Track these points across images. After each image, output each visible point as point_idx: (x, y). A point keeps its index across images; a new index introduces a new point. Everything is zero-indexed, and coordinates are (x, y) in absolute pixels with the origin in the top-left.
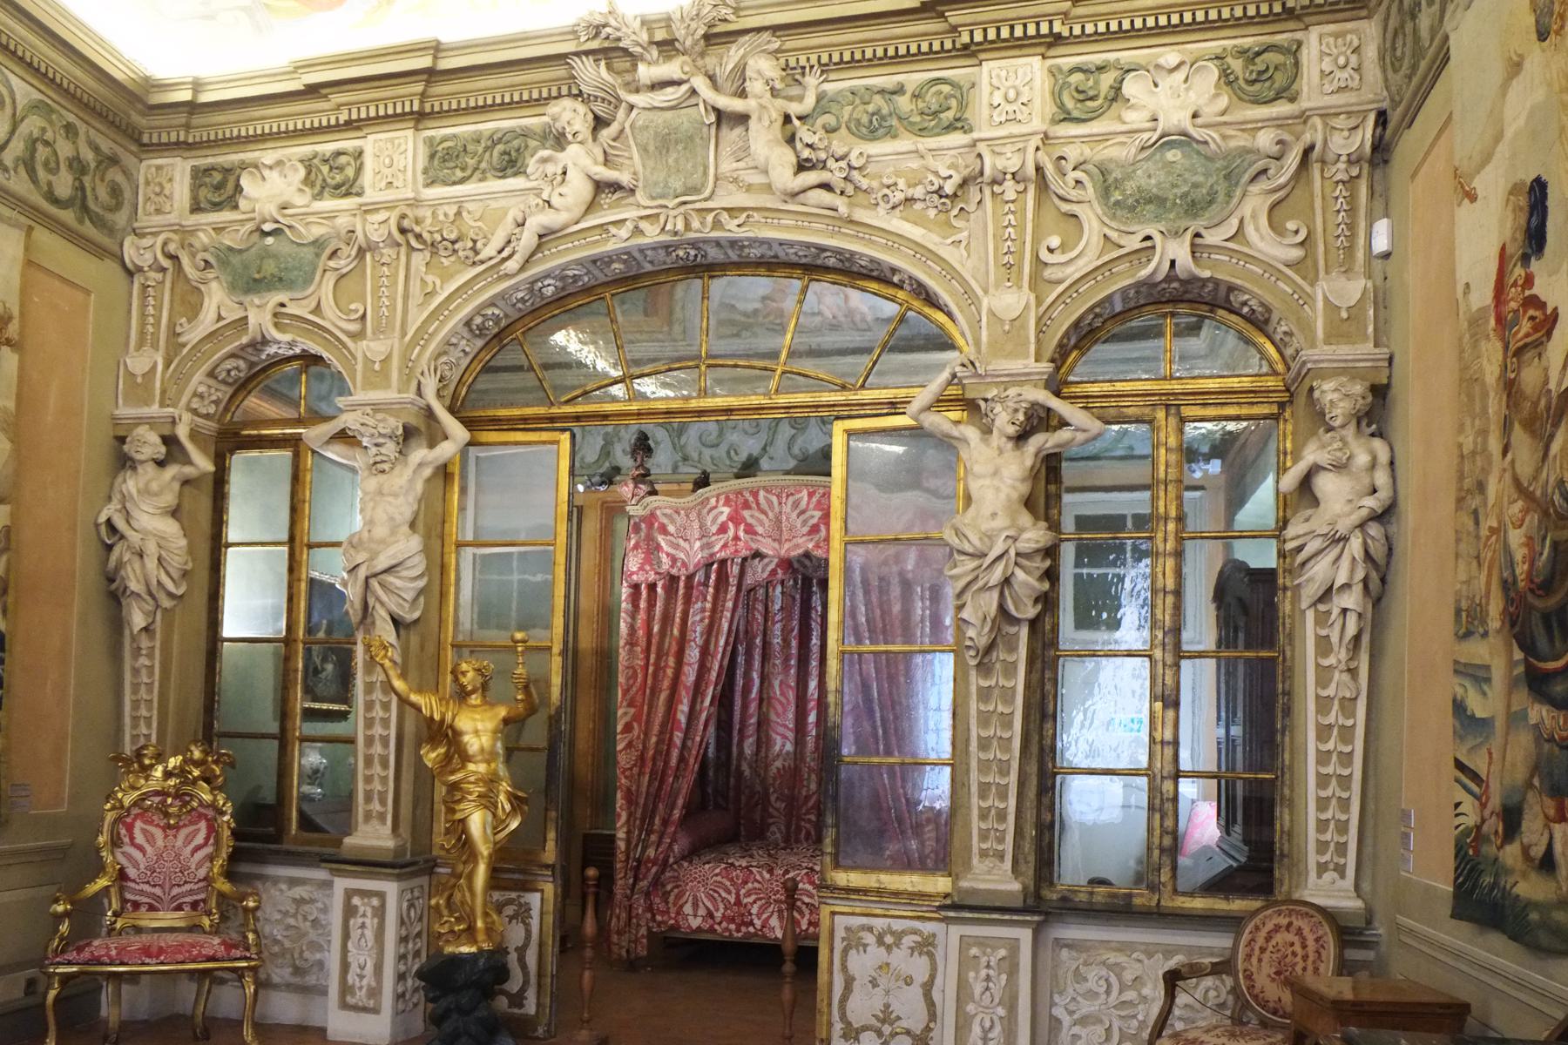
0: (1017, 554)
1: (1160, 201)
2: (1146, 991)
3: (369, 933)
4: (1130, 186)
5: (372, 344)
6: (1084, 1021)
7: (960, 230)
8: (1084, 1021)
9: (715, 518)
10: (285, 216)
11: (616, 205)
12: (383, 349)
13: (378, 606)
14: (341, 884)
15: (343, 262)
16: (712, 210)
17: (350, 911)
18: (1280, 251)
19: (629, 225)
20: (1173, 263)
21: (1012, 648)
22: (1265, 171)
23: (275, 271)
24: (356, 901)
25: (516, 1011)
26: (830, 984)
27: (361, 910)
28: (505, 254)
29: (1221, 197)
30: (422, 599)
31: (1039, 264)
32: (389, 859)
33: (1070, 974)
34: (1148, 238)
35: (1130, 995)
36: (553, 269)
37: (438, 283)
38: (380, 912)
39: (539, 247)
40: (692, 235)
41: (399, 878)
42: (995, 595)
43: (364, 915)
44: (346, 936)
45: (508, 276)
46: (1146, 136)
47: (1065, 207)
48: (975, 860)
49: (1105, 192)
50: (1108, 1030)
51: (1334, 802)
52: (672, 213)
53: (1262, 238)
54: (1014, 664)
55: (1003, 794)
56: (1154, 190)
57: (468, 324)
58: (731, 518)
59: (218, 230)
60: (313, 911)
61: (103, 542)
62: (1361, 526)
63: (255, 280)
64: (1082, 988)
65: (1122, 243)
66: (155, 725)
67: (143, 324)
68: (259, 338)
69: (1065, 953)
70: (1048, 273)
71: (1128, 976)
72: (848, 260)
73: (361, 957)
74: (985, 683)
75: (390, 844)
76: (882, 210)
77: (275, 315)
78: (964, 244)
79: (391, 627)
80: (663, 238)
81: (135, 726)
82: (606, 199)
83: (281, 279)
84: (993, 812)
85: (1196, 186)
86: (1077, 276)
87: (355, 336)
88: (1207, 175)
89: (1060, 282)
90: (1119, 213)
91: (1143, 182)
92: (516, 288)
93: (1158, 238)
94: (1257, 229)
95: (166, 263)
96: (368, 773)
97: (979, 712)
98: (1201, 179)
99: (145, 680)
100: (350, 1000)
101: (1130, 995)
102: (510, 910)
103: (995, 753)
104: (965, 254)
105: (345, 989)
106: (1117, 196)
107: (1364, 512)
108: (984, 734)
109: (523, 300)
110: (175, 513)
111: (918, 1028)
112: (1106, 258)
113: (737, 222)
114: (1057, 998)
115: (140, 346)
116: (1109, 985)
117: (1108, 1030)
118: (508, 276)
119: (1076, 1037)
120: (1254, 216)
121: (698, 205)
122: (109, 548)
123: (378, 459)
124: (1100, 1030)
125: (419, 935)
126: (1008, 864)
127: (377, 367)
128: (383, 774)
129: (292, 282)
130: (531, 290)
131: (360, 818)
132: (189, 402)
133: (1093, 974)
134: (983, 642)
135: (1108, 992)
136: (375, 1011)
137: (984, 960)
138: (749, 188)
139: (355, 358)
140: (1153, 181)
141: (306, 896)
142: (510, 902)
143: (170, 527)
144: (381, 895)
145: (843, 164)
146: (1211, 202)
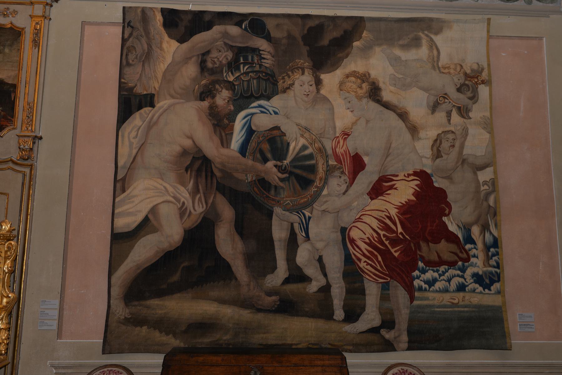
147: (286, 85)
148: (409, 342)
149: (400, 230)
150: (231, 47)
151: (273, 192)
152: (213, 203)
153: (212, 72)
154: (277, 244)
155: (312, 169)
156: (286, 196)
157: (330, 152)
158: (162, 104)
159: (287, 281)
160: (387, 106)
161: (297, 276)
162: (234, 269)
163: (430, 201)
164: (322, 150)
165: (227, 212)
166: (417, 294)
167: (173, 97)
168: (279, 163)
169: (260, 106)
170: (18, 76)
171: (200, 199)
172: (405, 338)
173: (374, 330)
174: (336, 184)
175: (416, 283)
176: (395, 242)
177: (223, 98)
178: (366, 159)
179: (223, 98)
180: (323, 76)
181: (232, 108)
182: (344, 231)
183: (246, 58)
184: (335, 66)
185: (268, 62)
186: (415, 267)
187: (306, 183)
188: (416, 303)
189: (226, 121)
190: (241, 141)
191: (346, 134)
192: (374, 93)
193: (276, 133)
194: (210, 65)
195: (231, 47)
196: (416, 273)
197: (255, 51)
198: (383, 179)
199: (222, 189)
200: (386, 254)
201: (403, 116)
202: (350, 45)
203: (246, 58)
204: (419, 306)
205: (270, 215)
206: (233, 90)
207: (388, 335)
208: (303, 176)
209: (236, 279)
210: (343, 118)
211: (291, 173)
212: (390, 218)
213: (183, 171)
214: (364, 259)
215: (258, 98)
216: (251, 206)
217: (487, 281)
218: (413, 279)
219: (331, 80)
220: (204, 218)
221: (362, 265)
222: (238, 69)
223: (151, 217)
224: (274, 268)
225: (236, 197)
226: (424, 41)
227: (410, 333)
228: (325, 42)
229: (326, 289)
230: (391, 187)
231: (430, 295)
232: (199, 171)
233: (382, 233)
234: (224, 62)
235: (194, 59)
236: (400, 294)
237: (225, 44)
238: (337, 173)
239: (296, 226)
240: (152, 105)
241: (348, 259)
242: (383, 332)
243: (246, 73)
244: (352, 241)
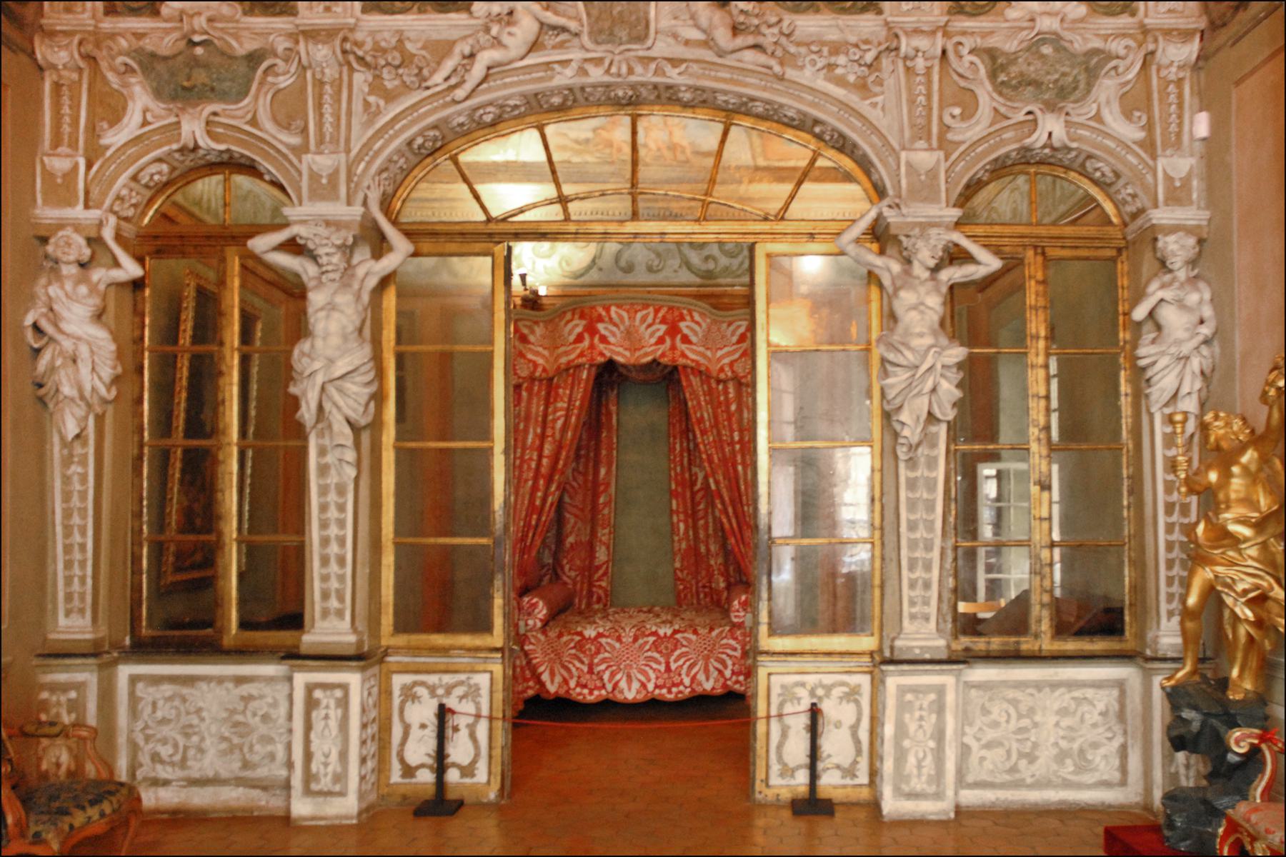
0: (943, 366)
1: (1036, 84)
2: (1038, 718)
3: (333, 724)
4: (1014, 70)
5: (318, 158)
6: (988, 746)
7: (876, 95)
8: (988, 746)
9: (654, 332)
10: (215, 28)
11: (561, 46)
12: (329, 162)
13: (335, 411)
14: (301, 679)
15: (281, 78)
16: (654, 59)
17: (311, 704)
18: (1131, 132)
19: (574, 65)
20: (1050, 134)
21: (934, 445)
22: (1115, 68)
23: (207, 81)
24: (318, 694)
25: (467, 780)
26: (768, 734)
27: (324, 702)
28: (453, 81)
29: (1082, 85)
30: (372, 405)
31: (945, 128)
32: (351, 651)
33: (978, 712)
34: (1030, 113)
35: (1025, 722)
36: (496, 99)
37: (382, 103)
38: (344, 703)
39: (485, 79)
40: (633, 78)
41: (363, 669)
42: (925, 400)
43: (327, 707)
44: (308, 727)
45: (455, 102)
46: (1025, 33)
47: (963, 83)
48: (906, 622)
49: (993, 75)
50: (1009, 752)
51: (1177, 562)
52: (617, 58)
53: (1115, 120)
54: (935, 459)
55: (928, 567)
56: (1033, 76)
57: (410, 143)
58: (667, 333)
59: (139, 36)
60: (261, 706)
61: (31, 347)
62: (1197, 348)
63: (184, 88)
64: (986, 719)
65: (1010, 115)
66: (90, 533)
68: (191, 145)
69: (974, 692)
70: (950, 136)
71: (1023, 708)
72: (775, 110)
73: (326, 745)
74: (912, 475)
75: (352, 638)
76: (808, 71)
77: (208, 123)
78: (880, 106)
79: (347, 430)
80: (607, 79)
82: (550, 40)
83: (213, 89)
84: (920, 582)
85: (1064, 74)
86: (975, 138)
87: (293, 149)
88: (1072, 66)
89: (963, 142)
90: (1005, 91)
91: (1024, 68)
92: (459, 113)
93: (1038, 113)
94: (1111, 113)
95: (82, 64)
96: (324, 571)
97: (908, 499)
98: (1067, 69)
99: (77, 487)
100: (314, 787)
101: (1025, 722)
102: (460, 691)
103: (920, 533)
104: (881, 114)
105: (309, 777)
106: (1002, 77)
107: (1201, 338)
108: (912, 517)
109: (462, 125)
110: (99, 316)
111: (846, 763)
112: (997, 127)
113: (677, 71)
114: (967, 729)
115: (56, 143)
116: (1009, 715)
117: (1009, 752)
118: (455, 102)
119: (982, 759)
120: (1108, 102)
121: (641, 53)
122: (37, 352)
123: (330, 268)
124: (1001, 752)
125: (374, 720)
126: (932, 624)
127: (324, 181)
128: (340, 572)
129: (225, 93)
130: (471, 116)
131: (317, 614)
132: (112, 205)
133: (997, 711)
134: (915, 440)
135: (1008, 722)
136: (342, 794)
137: (917, 704)
138: (687, 43)
139: (300, 174)
140: (1032, 68)
141: (255, 692)
142: (461, 683)
143: (100, 335)
144: (345, 687)
145: (775, 30)
146: (1075, 88)
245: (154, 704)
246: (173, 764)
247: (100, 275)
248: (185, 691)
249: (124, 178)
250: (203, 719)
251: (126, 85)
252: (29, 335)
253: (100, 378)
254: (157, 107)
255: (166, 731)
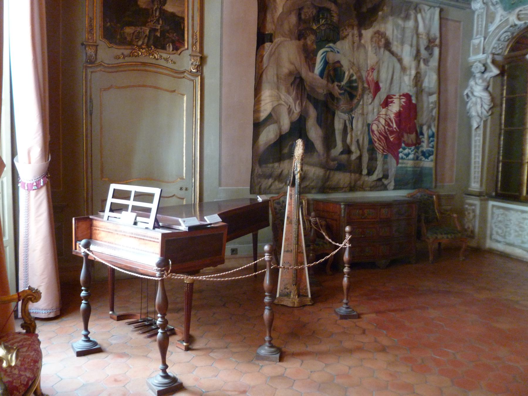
67: (478, 28)
81: (475, 158)
147: (344, 35)
148: (395, 186)
149: (395, 126)
150: (315, 7)
151: (336, 101)
152: (306, 107)
153: (305, 22)
154: (337, 132)
155: (356, 88)
156: (343, 105)
157: (364, 79)
158: (277, 40)
159: (342, 153)
160: (392, 53)
161: (347, 151)
162: (316, 146)
163: (410, 111)
164: (360, 77)
165: (312, 113)
166: (400, 161)
167: (283, 37)
168: (339, 84)
169: (330, 47)
170: (183, 12)
171: (299, 104)
172: (393, 184)
173: (380, 180)
174: (368, 98)
175: (400, 155)
176: (392, 132)
177: (310, 40)
178: (381, 85)
179: (310, 40)
180: (363, 32)
181: (315, 47)
182: (369, 125)
183: (323, 15)
184: (370, 25)
185: (335, 19)
186: (400, 146)
187: (352, 97)
188: (399, 165)
189: (312, 55)
190: (320, 69)
191: (373, 69)
192: (387, 45)
193: (338, 65)
194: (303, 17)
195: (315, 7)
196: (401, 150)
197: (329, 10)
198: (389, 97)
199: (309, 98)
200: (387, 138)
201: (400, 60)
202: (377, 13)
203: (323, 15)
204: (401, 167)
205: (334, 115)
206: (316, 36)
207: (386, 182)
208: (351, 92)
209: (317, 152)
210: (372, 59)
211: (345, 90)
212: (390, 119)
213: (289, 85)
214: (378, 142)
215: (329, 42)
216: (326, 109)
217: (427, 155)
218: (398, 153)
219: (368, 33)
220: (301, 115)
221: (377, 145)
222: (319, 22)
223: (273, 114)
224: (335, 146)
225: (316, 103)
226: (413, 17)
227: (395, 181)
228: (364, 10)
229: (360, 158)
230: (392, 102)
231: (405, 161)
232: (298, 86)
233: (386, 127)
234: (311, 16)
235: (295, 12)
236: (392, 161)
237: (312, 4)
238: (367, 92)
239: (347, 122)
240: (271, 41)
241: (371, 142)
242: (383, 180)
243: (323, 25)
244: (373, 131)
245: (498, 215)
246: (502, 236)
247: (487, 75)
248: (507, 213)
249: (494, 41)
250: (511, 223)
251: (496, 9)
252: (465, 97)
253: (485, 109)
254: (504, 13)
255: (500, 225)
